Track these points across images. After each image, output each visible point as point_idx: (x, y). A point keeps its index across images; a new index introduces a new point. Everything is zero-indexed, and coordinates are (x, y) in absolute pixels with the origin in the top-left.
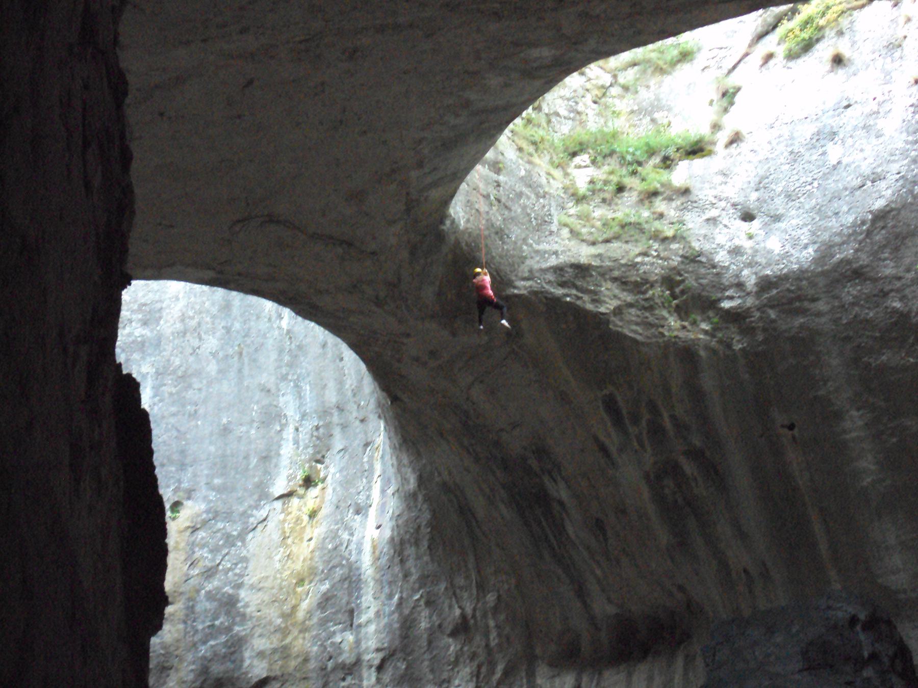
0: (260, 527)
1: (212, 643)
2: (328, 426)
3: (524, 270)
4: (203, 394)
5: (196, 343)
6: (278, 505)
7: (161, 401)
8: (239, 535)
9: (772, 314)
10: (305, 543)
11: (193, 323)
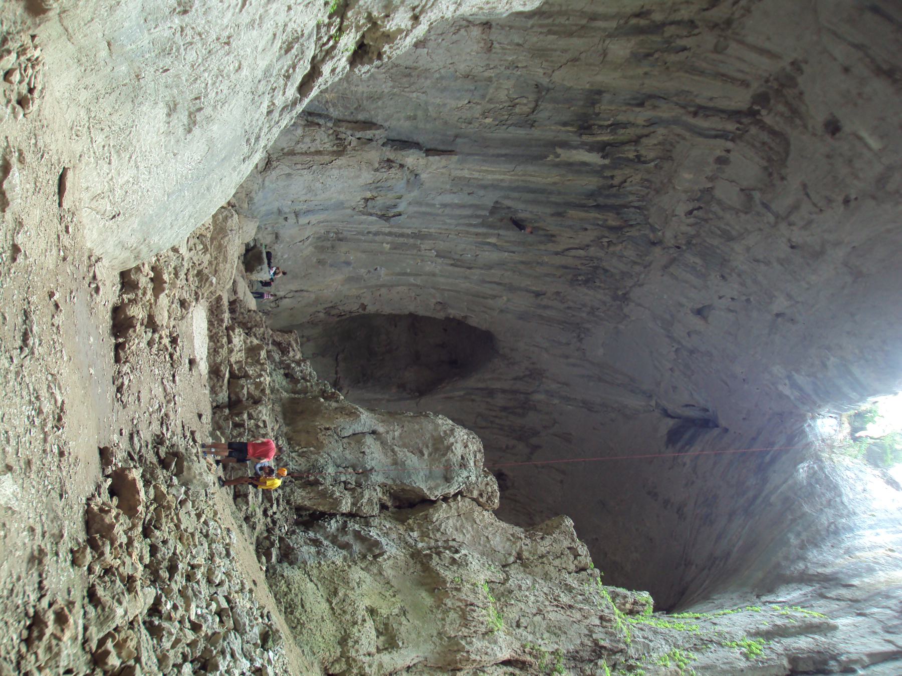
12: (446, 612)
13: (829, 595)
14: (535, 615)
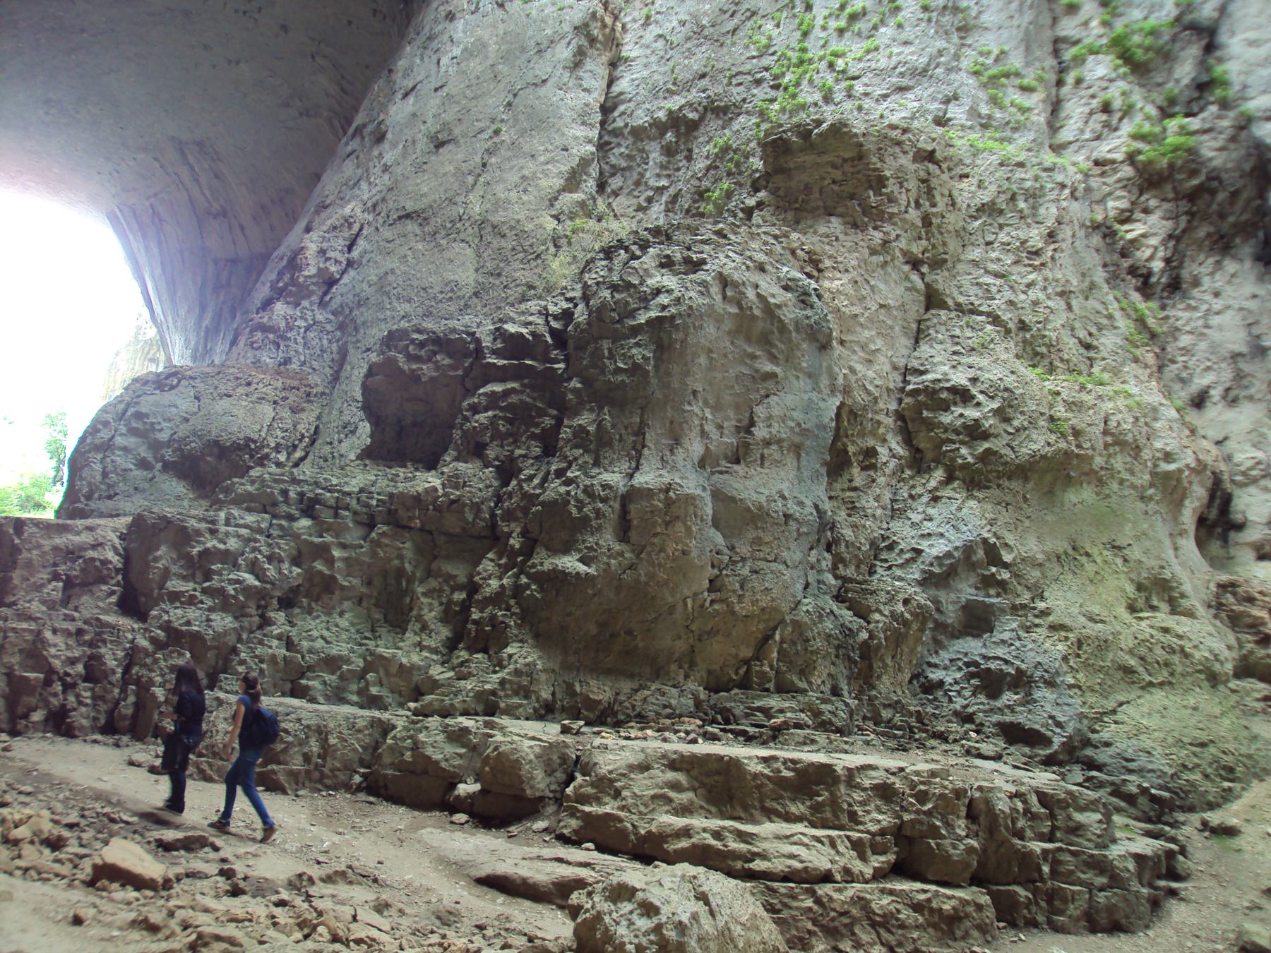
12: (1109, 469)
14: (1069, 307)
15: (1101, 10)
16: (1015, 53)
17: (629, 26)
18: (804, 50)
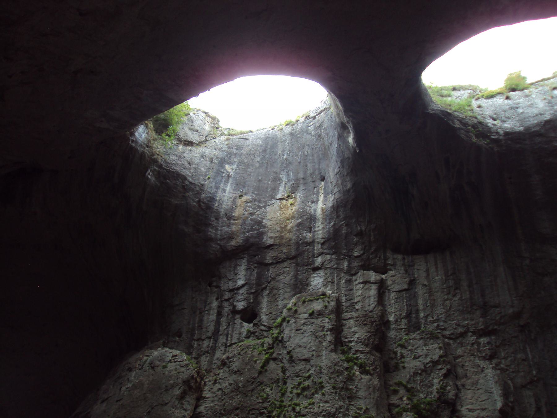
0: (271, 205)
1: (251, 233)
2: (297, 184)
3: (431, 107)
4: (253, 171)
5: (253, 158)
6: (278, 201)
7: (239, 169)
8: (263, 206)
9: (509, 142)
10: (289, 210)
11: (253, 152)
13: (268, 260)
15: (407, 393)
16: (373, 409)
17: (207, 383)
18: (282, 401)
